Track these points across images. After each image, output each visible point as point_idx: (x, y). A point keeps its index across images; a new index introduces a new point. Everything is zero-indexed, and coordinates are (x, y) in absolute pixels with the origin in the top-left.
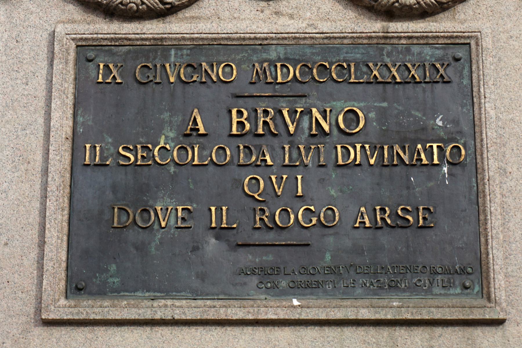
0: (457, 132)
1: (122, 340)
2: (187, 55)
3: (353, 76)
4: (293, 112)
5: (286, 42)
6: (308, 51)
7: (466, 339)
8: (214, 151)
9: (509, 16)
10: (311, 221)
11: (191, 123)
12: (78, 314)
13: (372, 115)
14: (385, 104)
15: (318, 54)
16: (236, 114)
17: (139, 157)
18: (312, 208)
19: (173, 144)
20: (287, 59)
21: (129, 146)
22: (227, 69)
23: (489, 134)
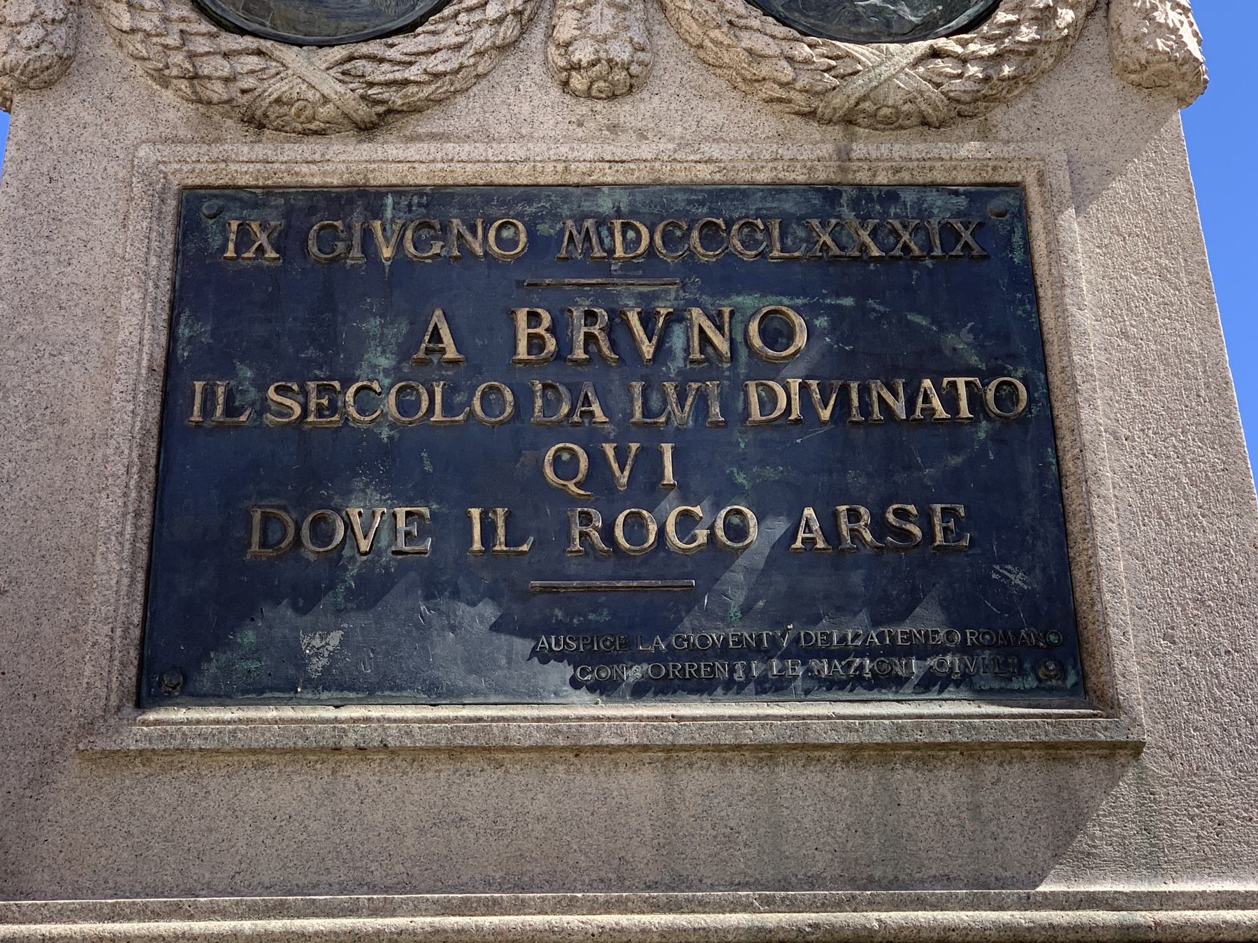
0: (1008, 356)
1: (264, 796)
2: (420, 205)
3: (778, 246)
4: (647, 320)
5: (632, 179)
6: (681, 197)
7: (1055, 790)
8: (478, 394)
9: (1100, 134)
10: (694, 539)
11: (427, 338)
12: (161, 738)
13: (822, 322)
14: (848, 302)
15: (702, 203)
16: (525, 318)
17: (312, 406)
18: (697, 510)
19: (387, 382)
20: (634, 213)
21: (289, 384)
22: (506, 234)
23: (1076, 358)
